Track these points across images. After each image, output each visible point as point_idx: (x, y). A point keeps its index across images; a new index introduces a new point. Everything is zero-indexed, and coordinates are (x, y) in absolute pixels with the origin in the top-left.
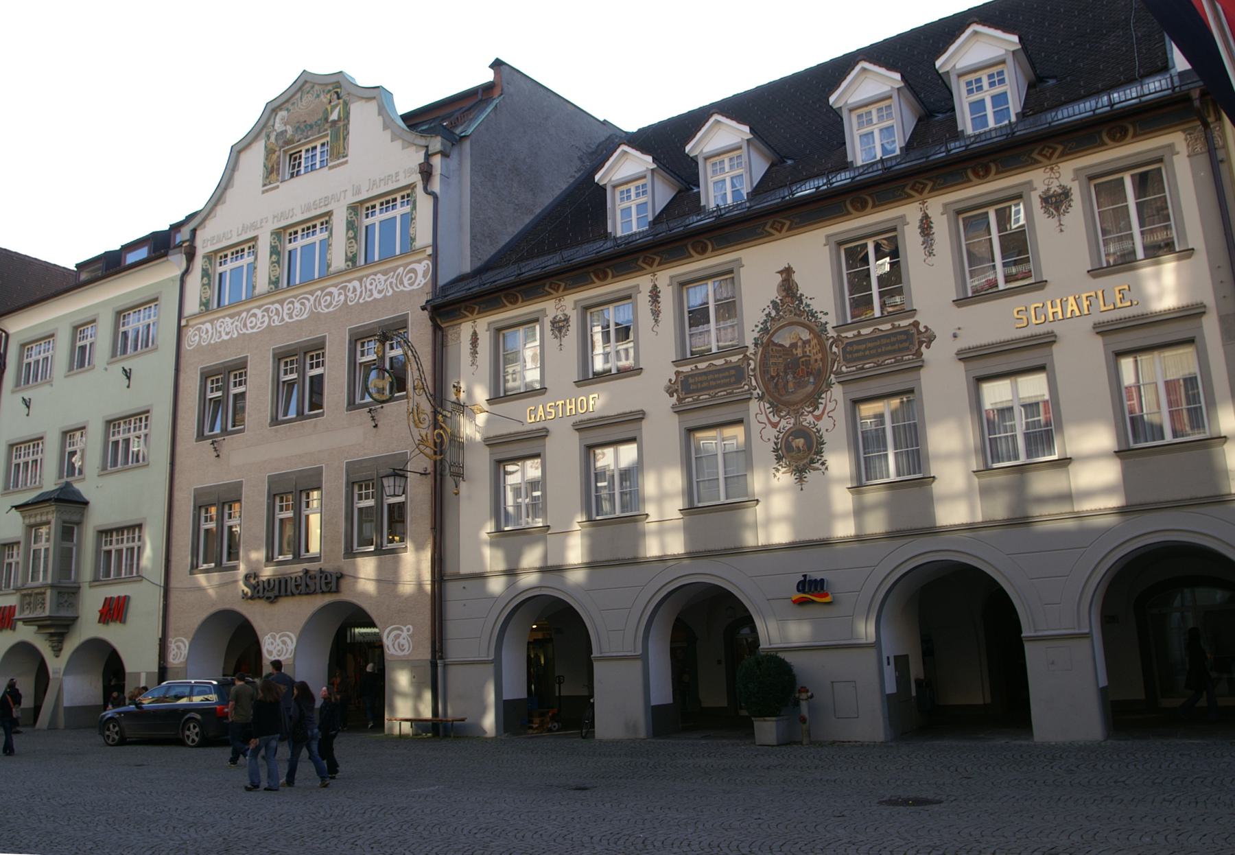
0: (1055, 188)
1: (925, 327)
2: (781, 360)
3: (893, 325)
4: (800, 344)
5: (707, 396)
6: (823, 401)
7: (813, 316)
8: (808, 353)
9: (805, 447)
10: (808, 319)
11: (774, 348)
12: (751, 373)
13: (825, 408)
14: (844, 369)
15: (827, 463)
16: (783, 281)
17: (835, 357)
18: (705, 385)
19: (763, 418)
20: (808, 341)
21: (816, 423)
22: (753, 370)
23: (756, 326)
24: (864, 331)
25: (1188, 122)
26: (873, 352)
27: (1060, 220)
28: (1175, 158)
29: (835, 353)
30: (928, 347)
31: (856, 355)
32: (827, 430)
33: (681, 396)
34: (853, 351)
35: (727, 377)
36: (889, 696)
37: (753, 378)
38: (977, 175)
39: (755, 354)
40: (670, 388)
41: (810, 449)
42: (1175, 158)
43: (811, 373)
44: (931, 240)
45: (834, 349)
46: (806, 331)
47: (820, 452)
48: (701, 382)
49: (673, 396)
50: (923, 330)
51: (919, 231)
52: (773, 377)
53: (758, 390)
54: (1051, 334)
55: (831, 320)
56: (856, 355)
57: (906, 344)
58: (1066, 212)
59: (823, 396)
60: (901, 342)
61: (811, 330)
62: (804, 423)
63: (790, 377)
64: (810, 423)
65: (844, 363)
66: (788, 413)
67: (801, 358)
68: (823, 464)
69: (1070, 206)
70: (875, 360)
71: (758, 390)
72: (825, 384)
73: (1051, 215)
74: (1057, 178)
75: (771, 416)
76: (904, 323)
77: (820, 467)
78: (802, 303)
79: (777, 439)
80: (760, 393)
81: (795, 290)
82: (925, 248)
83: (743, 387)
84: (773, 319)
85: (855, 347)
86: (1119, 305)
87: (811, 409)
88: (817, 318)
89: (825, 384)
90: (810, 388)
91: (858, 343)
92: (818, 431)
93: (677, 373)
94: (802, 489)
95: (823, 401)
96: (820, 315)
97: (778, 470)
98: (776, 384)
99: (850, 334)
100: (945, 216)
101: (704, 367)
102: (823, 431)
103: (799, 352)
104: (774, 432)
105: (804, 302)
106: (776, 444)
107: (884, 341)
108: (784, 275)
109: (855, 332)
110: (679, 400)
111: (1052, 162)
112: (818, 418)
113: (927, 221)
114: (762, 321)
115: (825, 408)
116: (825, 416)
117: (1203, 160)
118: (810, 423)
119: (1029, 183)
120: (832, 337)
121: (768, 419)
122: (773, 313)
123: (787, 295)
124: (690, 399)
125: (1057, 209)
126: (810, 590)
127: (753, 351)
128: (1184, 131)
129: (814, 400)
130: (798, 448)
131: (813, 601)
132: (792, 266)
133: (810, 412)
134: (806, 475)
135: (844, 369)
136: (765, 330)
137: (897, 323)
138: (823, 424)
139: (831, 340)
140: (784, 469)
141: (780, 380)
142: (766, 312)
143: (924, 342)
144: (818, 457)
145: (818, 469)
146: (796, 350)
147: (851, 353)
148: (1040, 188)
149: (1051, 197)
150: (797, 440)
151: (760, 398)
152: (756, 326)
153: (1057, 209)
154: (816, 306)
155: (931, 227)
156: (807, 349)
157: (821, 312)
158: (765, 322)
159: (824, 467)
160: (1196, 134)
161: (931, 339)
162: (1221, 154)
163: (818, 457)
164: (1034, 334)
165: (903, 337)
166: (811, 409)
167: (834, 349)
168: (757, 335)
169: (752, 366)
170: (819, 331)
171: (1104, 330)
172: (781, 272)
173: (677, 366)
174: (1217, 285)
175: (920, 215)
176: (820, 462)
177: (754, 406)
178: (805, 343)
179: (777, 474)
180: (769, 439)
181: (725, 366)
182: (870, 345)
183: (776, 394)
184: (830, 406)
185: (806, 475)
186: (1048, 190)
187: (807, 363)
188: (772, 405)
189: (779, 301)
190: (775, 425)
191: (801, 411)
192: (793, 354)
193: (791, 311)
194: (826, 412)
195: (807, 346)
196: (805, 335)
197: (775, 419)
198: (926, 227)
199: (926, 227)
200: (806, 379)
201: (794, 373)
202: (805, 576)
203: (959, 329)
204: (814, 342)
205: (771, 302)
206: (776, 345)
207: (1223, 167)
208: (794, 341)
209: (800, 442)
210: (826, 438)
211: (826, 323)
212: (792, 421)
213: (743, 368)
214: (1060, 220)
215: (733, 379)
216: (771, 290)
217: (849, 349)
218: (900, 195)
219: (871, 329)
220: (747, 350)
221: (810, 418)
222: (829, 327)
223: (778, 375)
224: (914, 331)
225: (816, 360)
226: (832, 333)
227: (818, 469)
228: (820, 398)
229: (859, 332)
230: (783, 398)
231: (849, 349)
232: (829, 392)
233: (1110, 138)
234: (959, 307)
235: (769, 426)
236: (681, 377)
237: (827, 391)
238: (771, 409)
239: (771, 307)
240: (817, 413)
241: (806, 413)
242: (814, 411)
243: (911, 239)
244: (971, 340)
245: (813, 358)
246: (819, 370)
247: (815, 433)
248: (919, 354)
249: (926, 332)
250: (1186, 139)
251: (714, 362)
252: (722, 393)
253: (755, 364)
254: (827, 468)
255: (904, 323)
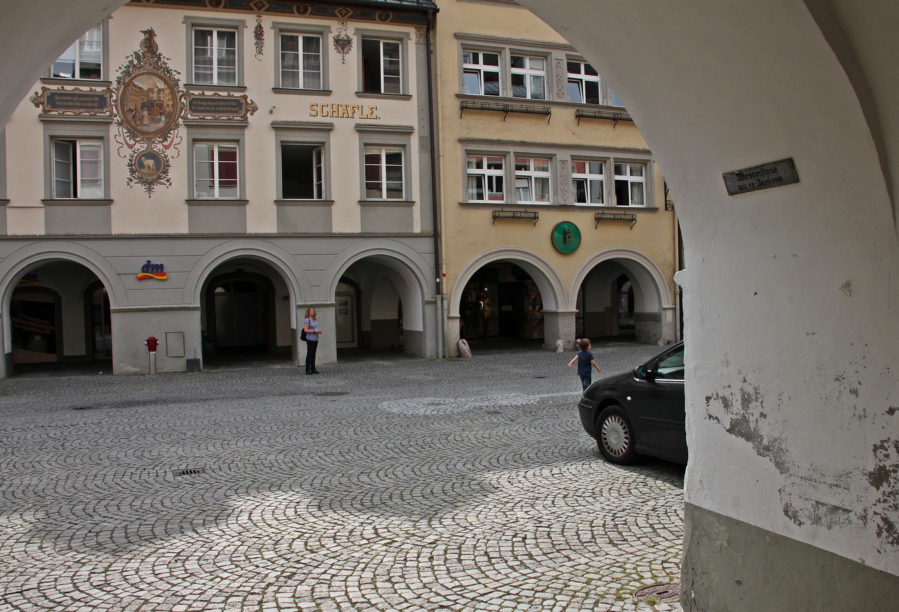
0: (342, 36)
1: (251, 101)
2: (138, 99)
3: (229, 93)
4: (156, 90)
5: (71, 113)
6: (172, 136)
7: (168, 72)
8: (162, 99)
9: (154, 166)
10: (166, 75)
11: (134, 88)
12: (113, 103)
13: (172, 141)
14: (189, 116)
15: (171, 181)
16: (145, 39)
17: (183, 106)
18: (70, 104)
19: (121, 139)
20: (163, 90)
21: (164, 150)
22: (115, 101)
23: (120, 68)
24: (207, 93)
25: (420, 24)
26: (213, 109)
27: (343, 57)
28: (409, 41)
29: (183, 103)
30: (252, 114)
31: (198, 108)
32: (173, 157)
33: (47, 109)
34: (197, 105)
35: (91, 102)
36: (8, 354)
37: (114, 107)
38: (298, 11)
39: (117, 89)
40: (36, 99)
41: (158, 169)
42: (409, 41)
43: (163, 114)
44: (262, 43)
45: (183, 100)
46: (162, 82)
47: (166, 172)
48: (67, 101)
49: (39, 107)
50: (250, 102)
51: (254, 34)
52: (131, 111)
53: (118, 118)
54: (332, 125)
55: (183, 80)
56: (198, 108)
57: (237, 109)
58: (347, 52)
59: (172, 132)
60: (234, 106)
61: (166, 82)
62: (155, 149)
63: (145, 113)
64: (159, 150)
65: (190, 112)
66: (143, 139)
67: (155, 101)
68: (168, 181)
69: (350, 49)
70: (213, 115)
71: (118, 118)
72: (173, 124)
73: (339, 52)
74: (345, 30)
75: (128, 139)
76: (237, 94)
77: (166, 182)
78: (160, 60)
79: (132, 157)
80: (120, 120)
81: (155, 49)
82: (257, 47)
83: (105, 113)
84: (134, 66)
85: (199, 103)
86: (369, 116)
87: (161, 140)
88: (171, 74)
89: (173, 124)
90: (161, 125)
91: (201, 100)
92: (166, 157)
93: (44, 89)
94: (150, 197)
95: (172, 136)
96: (174, 73)
97: (131, 180)
98: (134, 117)
99: (196, 93)
100: (185, 25)
101: (70, 89)
102: (169, 157)
103: (154, 96)
104: (130, 151)
105: (162, 60)
106: (131, 160)
107: (221, 103)
108: (147, 35)
109: (201, 92)
110: (45, 111)
111: (343, 19)
112: (167, 147)
113: (260, 29)
114: (125, 65)
115: (172, 141)
116: (172, 147)
117: (423, 48)
118: (159, 150)
119: (329, 27)
120: (183, 91)
121: (126, 141)
122: (136, 62)
123: (149, 51)
124: (56, 113)
125: (343, 49)
126: (152, 271)
127: (116, 87)
128: (416, 28)
129: (164, 134)
130: (149, 167)
131: (151, 278)
132: (154, 30)
133: (160, 142)
134: (154, 187)
135: (189, 116)
136: (127, 73)
137: (232, 93)
138: (170, 153)
139: (181, 93)
140: (136, 180)
141: (137, 114)
142: (130, 59)
143: (249, 110)
144: (164, 175)
145: (164, 184)
146: (152, 94)
147: (196, 106)
148: (335, 33)
149: (340, 40)
150: (148, 160)
151: (120, 124)
152: (120, 68)
153: (343, 49)
154: (171, 65)
155: (263, 35)
156: (161, 95)
157: (175, 71)
158: (128, 67)
159: (168, 183)
160: (421, 32)
161: (255, 109)
162: (432, 48)
163: (164, 175)
164: (321, 122)
165: (236, 104)
166: (161, 140)
167: (183, 100)
168: (120, 75)
169: (114, 97)
170: (172, 84)
171: (361, 130)
172: (144, 32)
173: (44, 83)
174: (420, 119)
175: (255, 24)
176: (165, 179)
177: (114, 129)
178: (160, 90)
179: (130, 183)
180: (125, 156)
181: (90, 93)
182: (212, 104)
183: (133, 124)
184: (176, 141)
185: (154, 187)
186: (339, 35)
187: (161, 106)
188: (129, 131)
189: (141, 54)
190: (131, 147)
191: (153, 140)
192: (150, 97)
193: (150, 64)
194: (173, 144)
195: (162, 93)
196: (161, 85)
197: (132, 142)
198: (259, 33)
199: (259, 33)
200: (159, 117)
201: (149, 110)
202: (149, 262)
203: (274, 107)
204: (168, 91)
205: (134, 53)
206: (135, 86)
207: (432, 56)
208: (150, 87)
209: (150, 162)
210: (171, 162)
211: (179, 80)
212: (145, 146)
213: (106, 98)
214: (343, 57)
215: (96, 105)
216: (136, 44)
217: (194, 102)
218: (330, 13)
219: (212, 93)
220: (110, 85)
221: (160, 146)
222: (181, 84)
223: (136, 109)
224: (243, 101)
225: (168, 105)
226: (182, 88)
227: (164, 184)
228: (169, 133)
229: (203, 93)
230: (138, 127)
231: (194, 102)
232: (176, 131)
233: (379, 17)
234: (275, 93)
235: (125, 146)
236: (47, 94)
237: (175, 129)
238: (128, 134)
239: (134, 57)
240: (165, 143)
241: (157, 142)
242: (164, 141)
243: (248, 37)
244: (282, 116)
245: (166, 103)
246: (170, 113)
247: (163, 157)
248: (245, 118)
249: (251, 104)
250: (416, 33)
251: (81, 88)
252: (225, 118)
253: (117, 97)
254: (170, 184)
255: (237, 94)
